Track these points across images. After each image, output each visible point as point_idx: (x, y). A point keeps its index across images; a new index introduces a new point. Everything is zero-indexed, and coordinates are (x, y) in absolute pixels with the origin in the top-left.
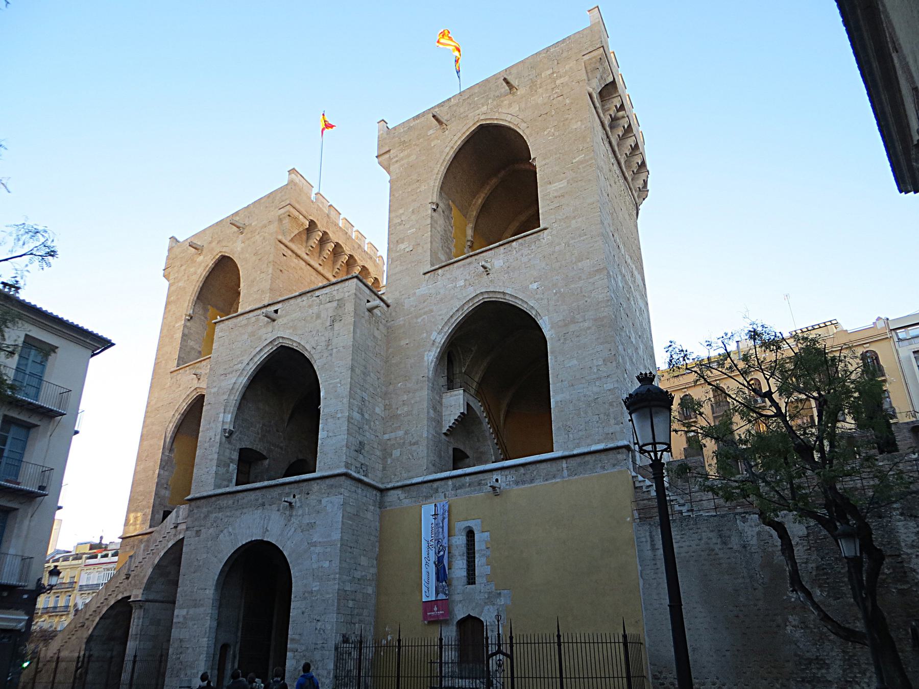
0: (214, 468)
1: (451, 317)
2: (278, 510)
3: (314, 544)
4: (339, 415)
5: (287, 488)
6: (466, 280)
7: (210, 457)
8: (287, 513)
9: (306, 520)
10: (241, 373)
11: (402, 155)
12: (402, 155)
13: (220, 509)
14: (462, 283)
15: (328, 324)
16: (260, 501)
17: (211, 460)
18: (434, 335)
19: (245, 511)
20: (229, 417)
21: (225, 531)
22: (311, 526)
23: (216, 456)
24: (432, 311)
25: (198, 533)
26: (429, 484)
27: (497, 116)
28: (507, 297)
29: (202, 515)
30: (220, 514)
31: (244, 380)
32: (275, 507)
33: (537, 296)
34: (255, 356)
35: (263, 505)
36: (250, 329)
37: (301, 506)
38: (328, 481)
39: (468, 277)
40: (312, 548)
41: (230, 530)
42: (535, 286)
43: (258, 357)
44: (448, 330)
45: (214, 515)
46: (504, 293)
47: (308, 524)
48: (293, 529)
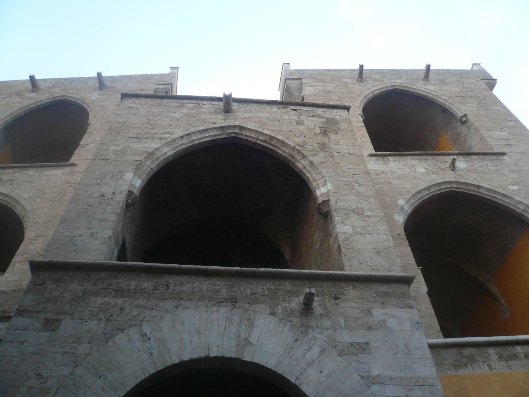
0: (110, 232)
1: (419, 192)
2: (273, 314)
3: (380, 381)
4: (369, 213)
5: (288, 285)
6: (426, 169)
7: (99, 216)
8: (297, 321)
9: (345, 337)
10: (169, 143)
11: (316, 84)
12: (316, 84)
13: (120, 292)
14: (423, 170)
15: (318, 131)
16: (224, 293)
17: (101, 220)
18: (401, 202)
19: (183, 303)
20: (138, 183)
21: (133, 332)
22: (363, 348)
23: (115, 218)
24: (390, 183)
25: (51, 325)
26: (455, 350)
27: (414, 87)
28: (482, 191)
29: (68, 296)
30: (119, 301)
31: (168, 152)
32: (263, 309)
33: (522, 195)
34: (194, 133)
35: (233, 301)
36: (185, 111)
37: (327, 314)
38: (376, 287)
39: (427, 167)
40: (375, 388)
41: (146, 329)
42: (515, 188)
43: (199, 136)
44: (415, 202)
45: (100, 300)
46: (478, 187)
47: (351, 344)
48: (316, 350)
